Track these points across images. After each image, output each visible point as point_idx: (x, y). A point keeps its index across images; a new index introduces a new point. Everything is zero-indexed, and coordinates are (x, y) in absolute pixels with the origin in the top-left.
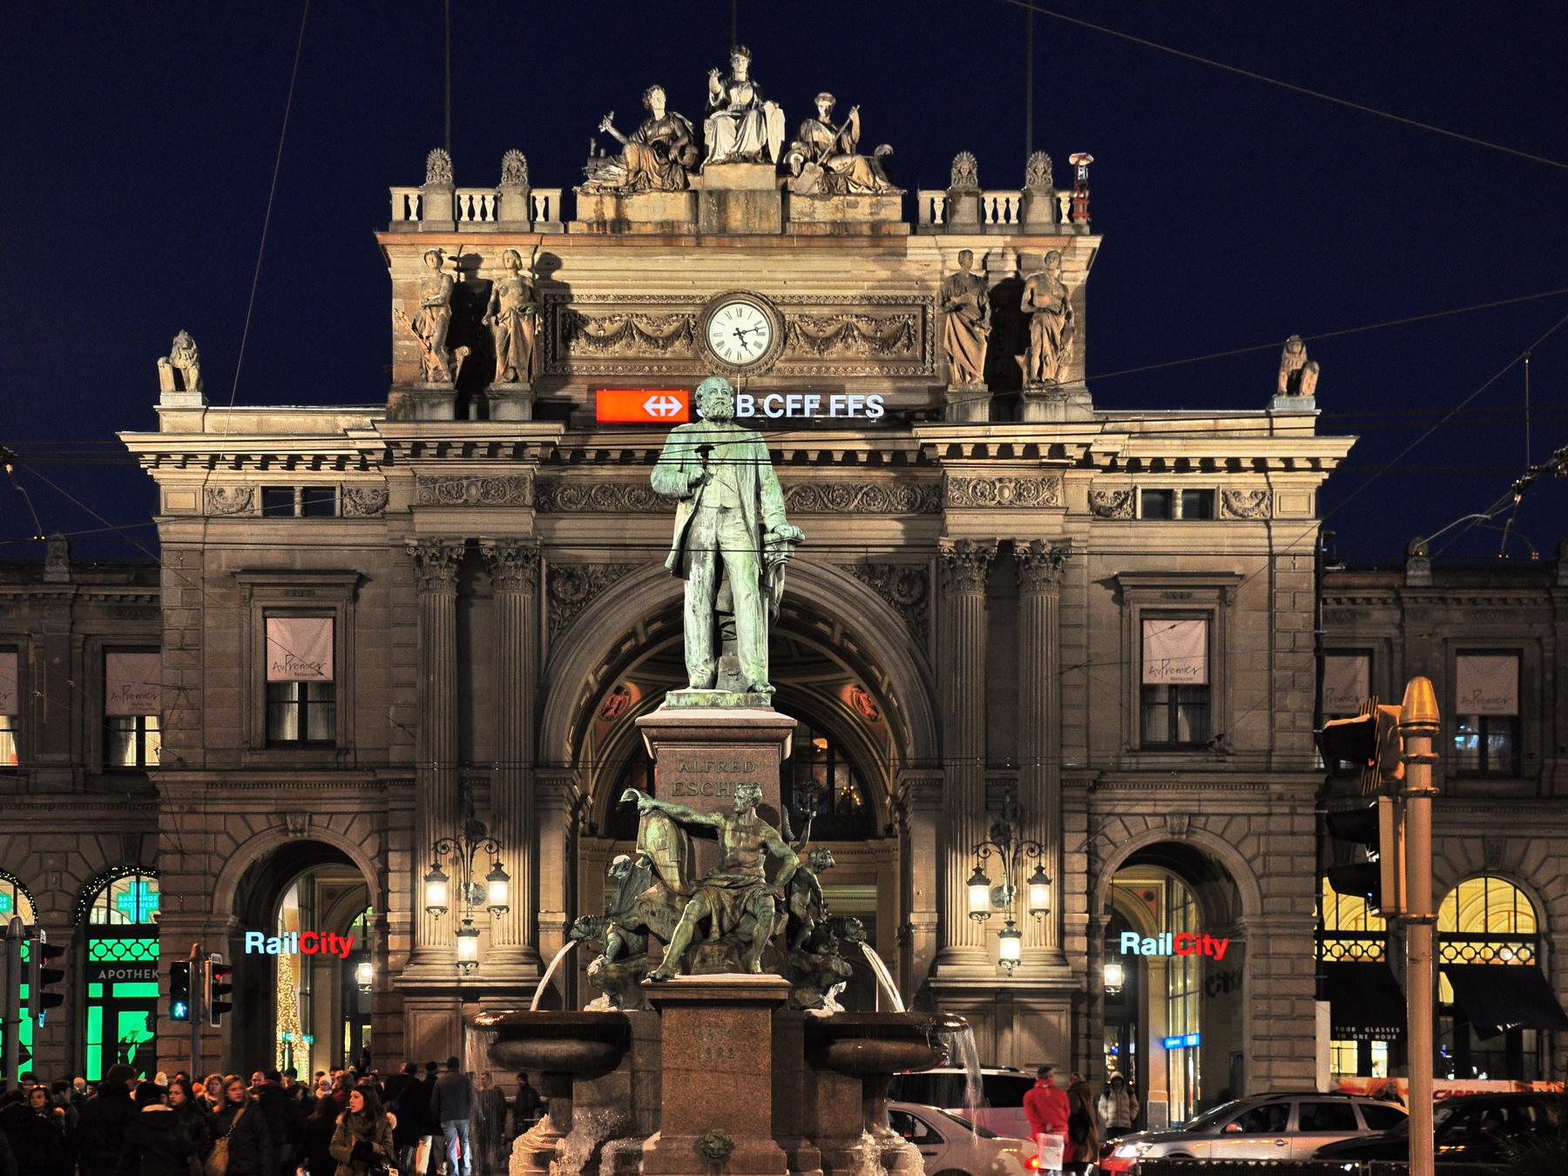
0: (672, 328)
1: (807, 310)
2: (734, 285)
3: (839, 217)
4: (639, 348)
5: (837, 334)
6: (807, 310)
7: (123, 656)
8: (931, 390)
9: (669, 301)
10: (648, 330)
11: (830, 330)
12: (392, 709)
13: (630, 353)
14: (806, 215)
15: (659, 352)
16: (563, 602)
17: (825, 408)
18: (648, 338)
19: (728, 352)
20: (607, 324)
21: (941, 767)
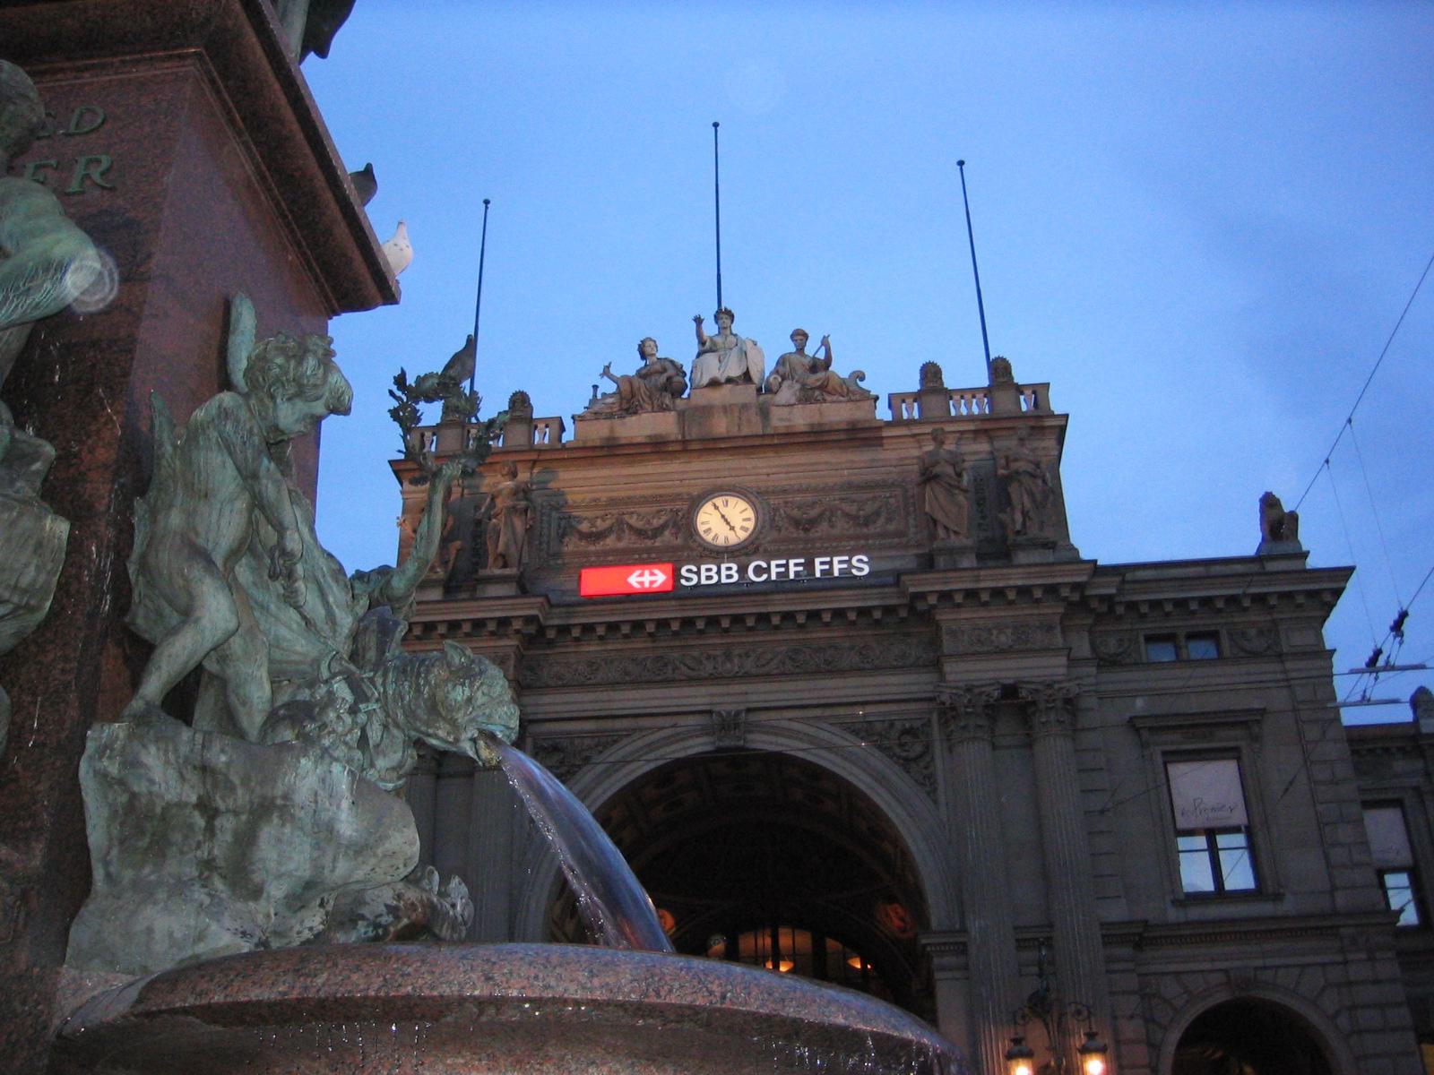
0: (661, 521)
1: (790, 498)
2: (719, 482)
3: (816, 419)
4: (628, 541)
5: (821, 515)
6: (790, 498)
8: (918, 556)
9: (657, 499)
10: (639, 524)
11: (813, 513)
13: (621, 545)
14: (789, 420)
15: (649, 543)
18: (640, 533)
19: (716, 537)
20: (599, 522)
21: (964, 931)
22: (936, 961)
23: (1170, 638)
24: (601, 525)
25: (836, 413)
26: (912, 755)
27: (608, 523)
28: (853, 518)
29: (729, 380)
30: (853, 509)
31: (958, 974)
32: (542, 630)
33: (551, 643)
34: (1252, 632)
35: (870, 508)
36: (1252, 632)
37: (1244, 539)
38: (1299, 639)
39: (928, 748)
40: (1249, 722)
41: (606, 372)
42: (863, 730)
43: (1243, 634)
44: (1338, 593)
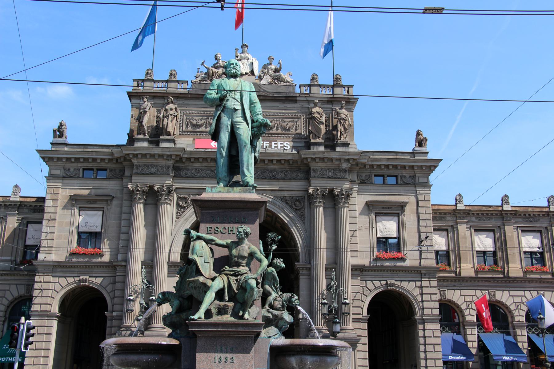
7: (33, 225)
8: (305, 142)
12: (120, 241)
16: (182, 207)
17: (270, 146)
22: (301, 272)
23: (383, 176)
24: (200, 122)
25: (282, 89)
26: (298, 208)
27: (203, 121)
28: (284, 129)
29: (246, 74)
30: (285, 124)
31: (307, 277)
32: (181, 159)
33: (184, 163)
34: (408, 177)
35: (290, 125)
36: (408, 177)
37: (409, 145)
38: (422, 180)
39: (303, 207)
40: (402, 206)
41: (202, 64)
42: (284, 199)
43: (405, 177)
44: (435, 167)
